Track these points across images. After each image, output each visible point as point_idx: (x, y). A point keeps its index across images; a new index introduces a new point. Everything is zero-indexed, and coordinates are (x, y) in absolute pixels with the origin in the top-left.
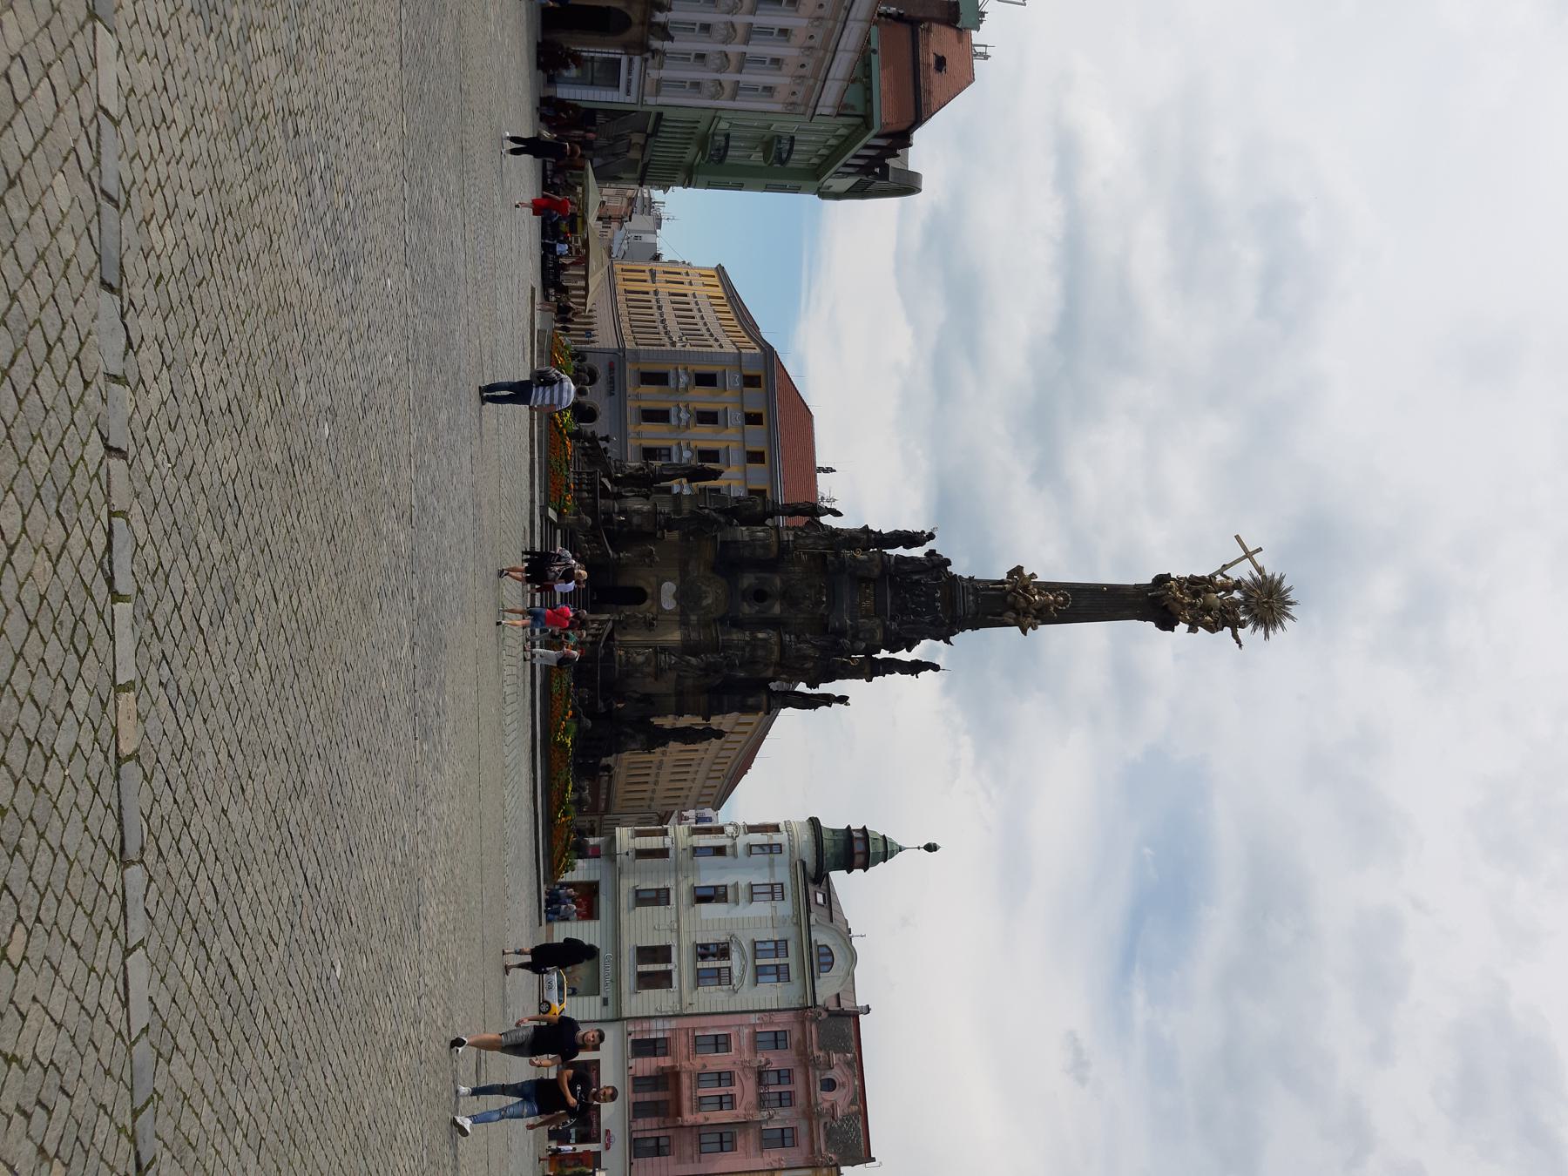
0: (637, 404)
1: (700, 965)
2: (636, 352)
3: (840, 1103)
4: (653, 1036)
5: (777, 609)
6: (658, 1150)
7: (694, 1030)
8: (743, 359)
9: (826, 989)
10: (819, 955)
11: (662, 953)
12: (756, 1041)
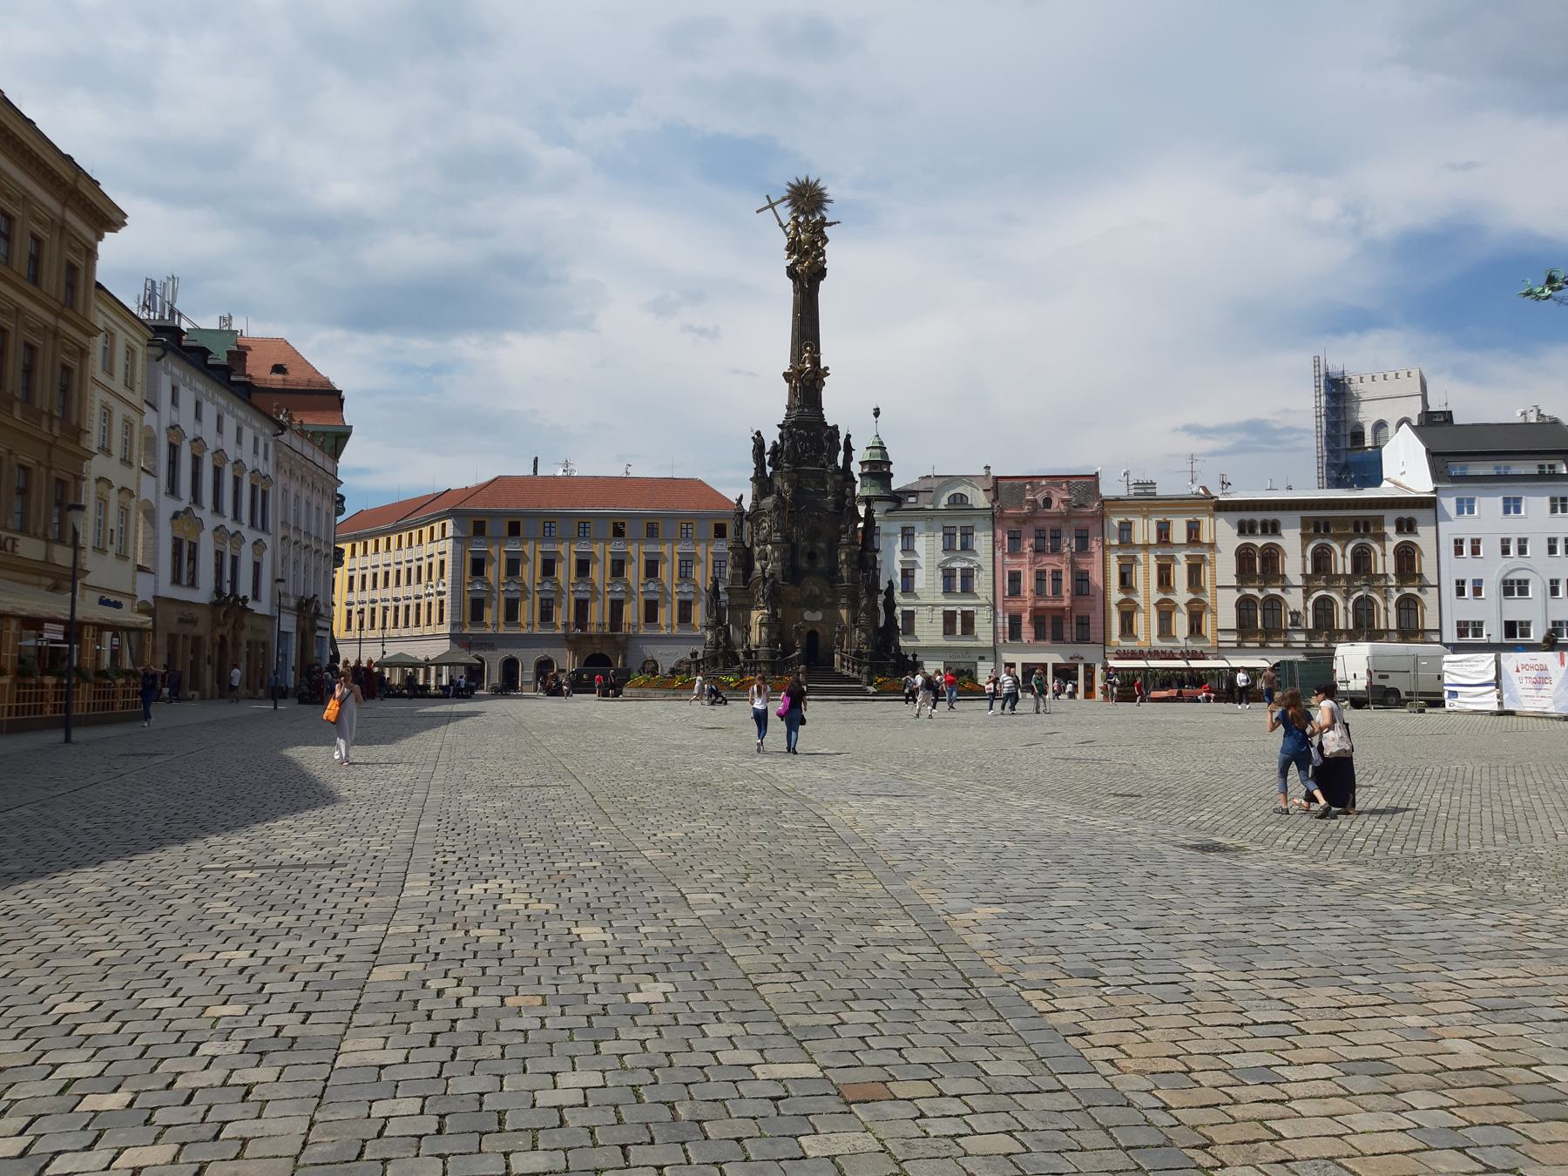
0: (502, 626)
1: (959, 591)
2: (453, 625)
3: (1059, 495)
4: (1007, 625)
5: (822, 545)
6: (1083, 623)
7: (1004, 596)
8: (459, 534)
9: (980, 499)
10: (955, 503)
11: (949, 618)
12: (1015, 551)
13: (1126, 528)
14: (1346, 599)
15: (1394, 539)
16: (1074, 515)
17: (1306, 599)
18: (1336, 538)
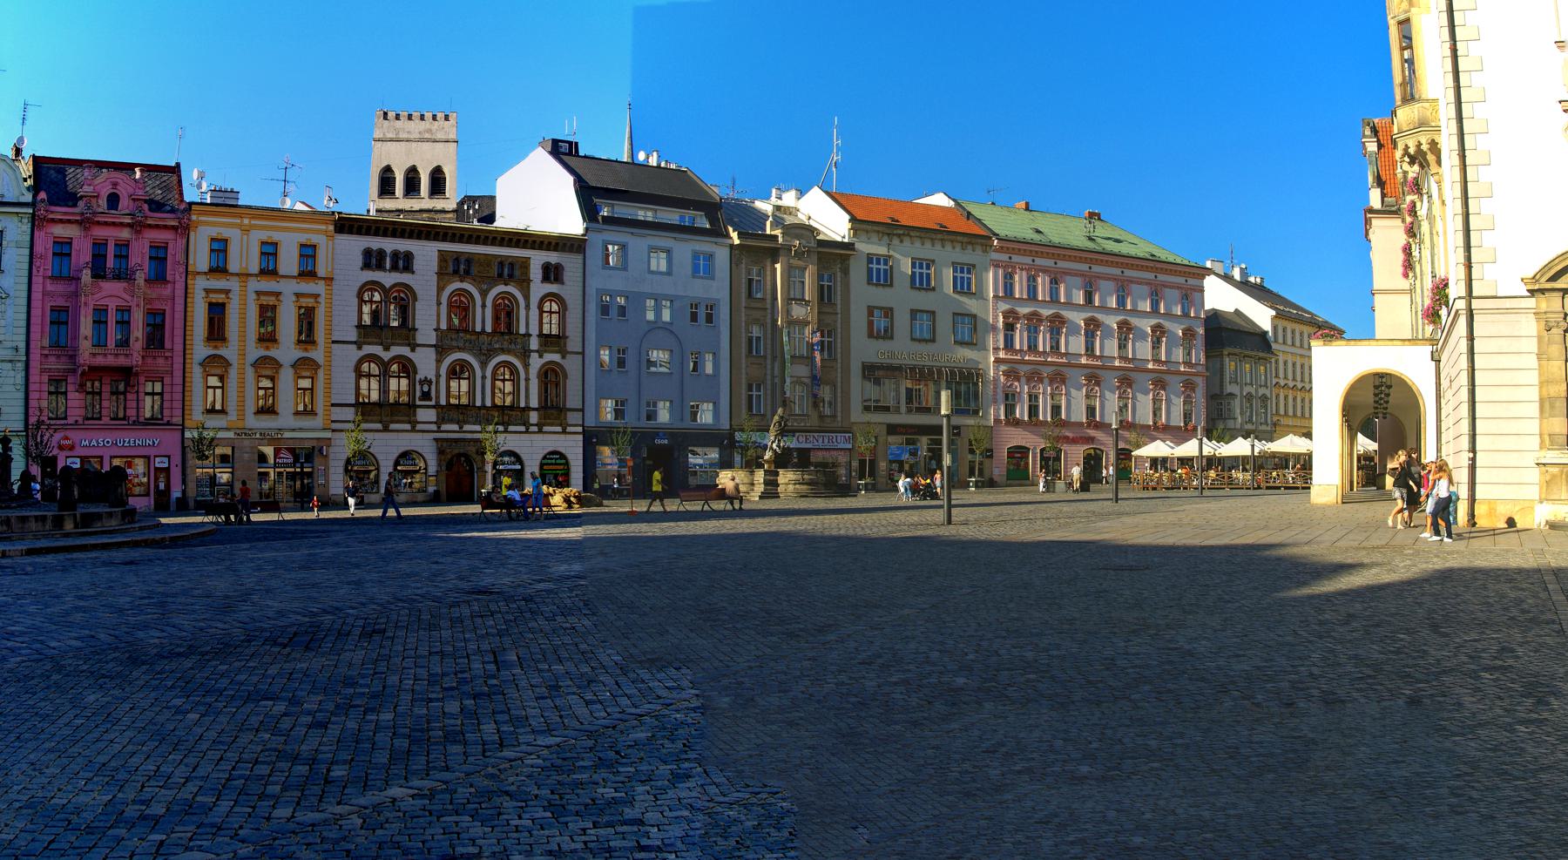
7: (43, 348)
13: (220, 248)
14: (484, 365)
15: (539, 288)
16: (150, 222)
17: (439, 362)
18: (476, 281)
